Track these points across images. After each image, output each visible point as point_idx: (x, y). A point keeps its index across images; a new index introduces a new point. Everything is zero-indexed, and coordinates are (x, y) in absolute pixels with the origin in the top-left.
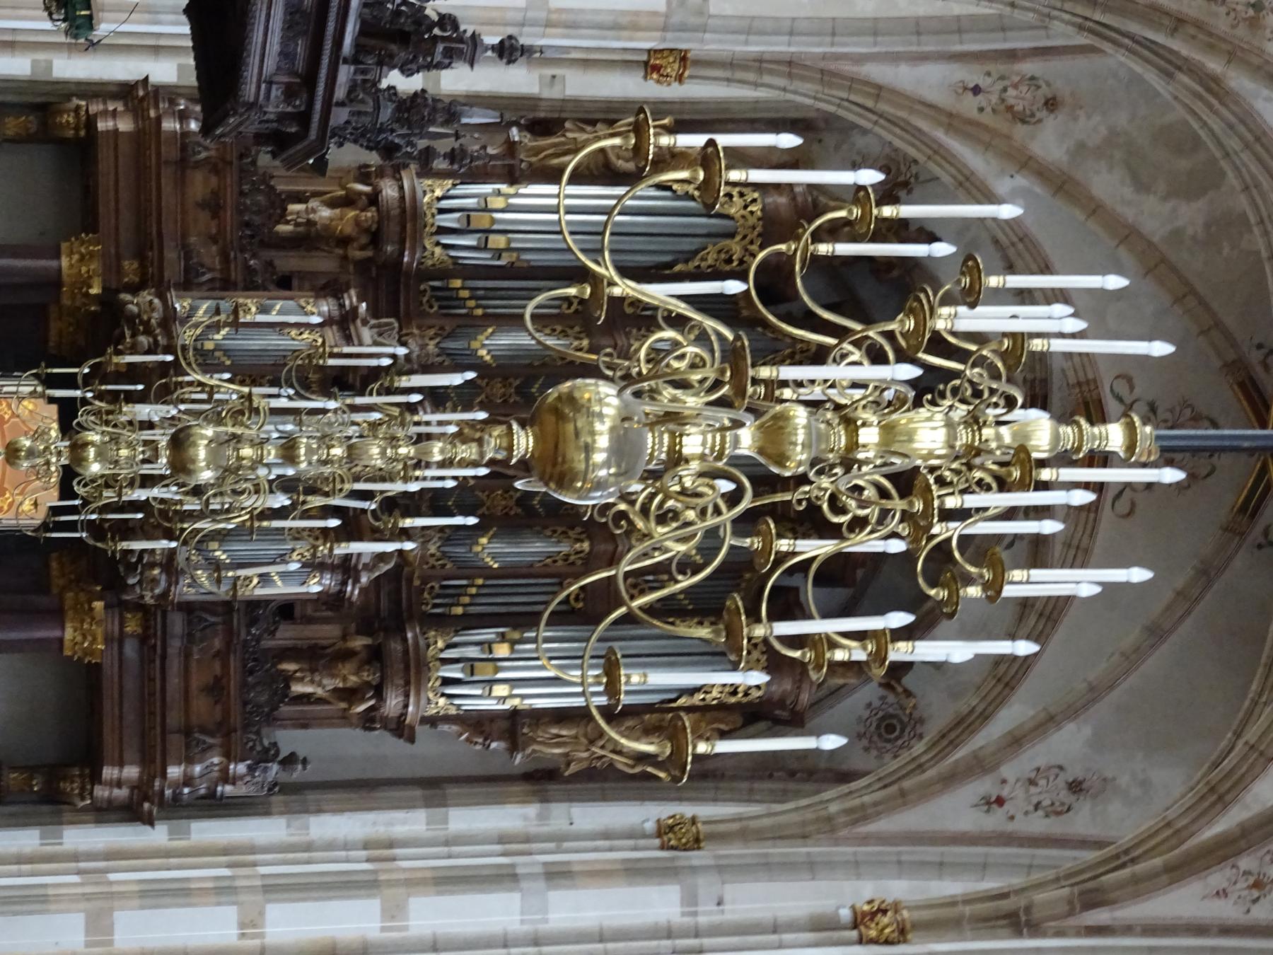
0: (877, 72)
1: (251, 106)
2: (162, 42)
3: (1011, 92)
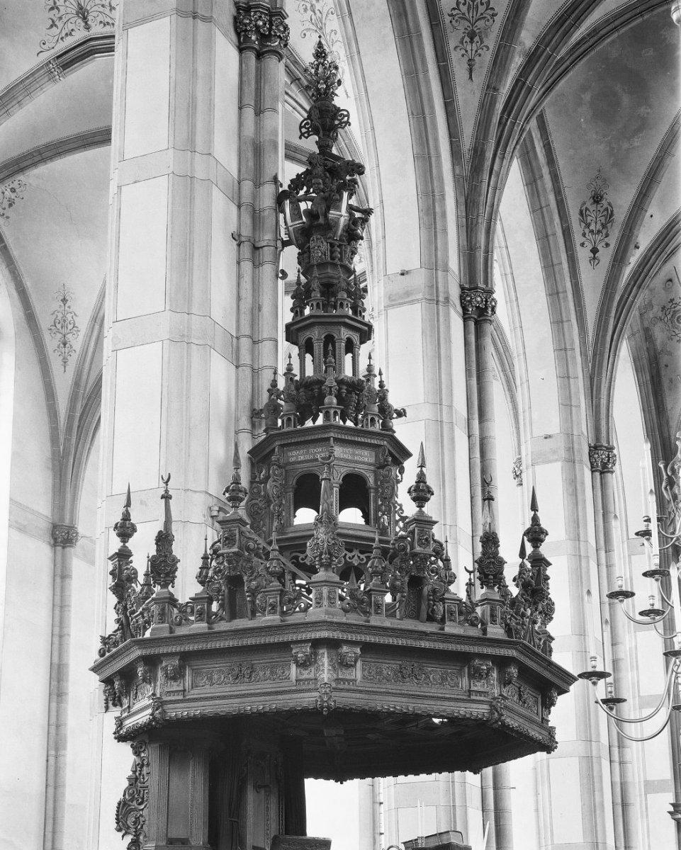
1: (493, 708)
2: (619, 800)
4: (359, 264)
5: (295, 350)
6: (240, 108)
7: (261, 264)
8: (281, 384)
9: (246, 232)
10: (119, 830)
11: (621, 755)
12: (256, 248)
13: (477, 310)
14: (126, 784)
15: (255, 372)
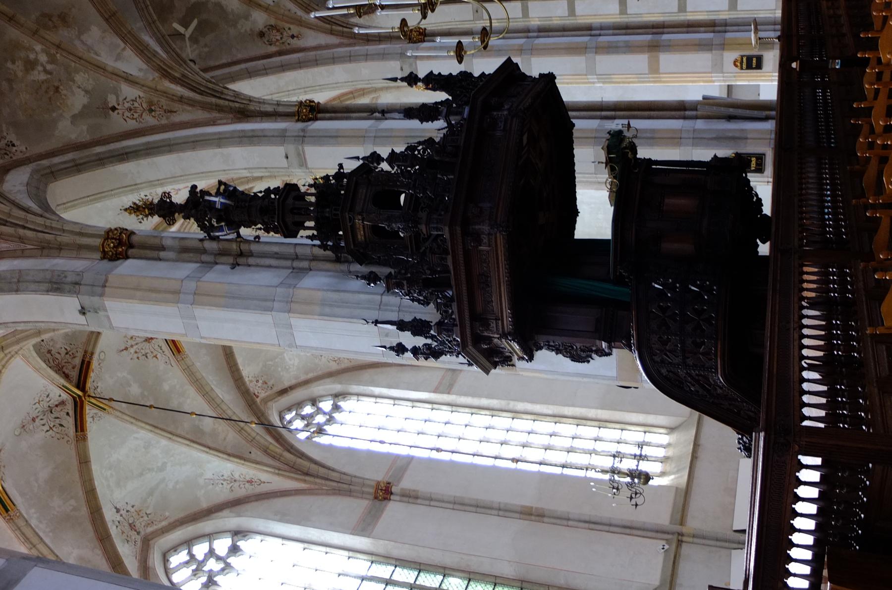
0: (334, 40)
2: (624, 31)
3: (278, 38)
4: (258, 187)
5: (302, 233)
6: (160, 260)
7: (251, 252)
8: (317, 242)
9: (231, 260)
10: (588, 362)
11: (596, 29)
12: (241, 254)
13: (311, 111)
14: (560, 356)
15: (315, 258)
